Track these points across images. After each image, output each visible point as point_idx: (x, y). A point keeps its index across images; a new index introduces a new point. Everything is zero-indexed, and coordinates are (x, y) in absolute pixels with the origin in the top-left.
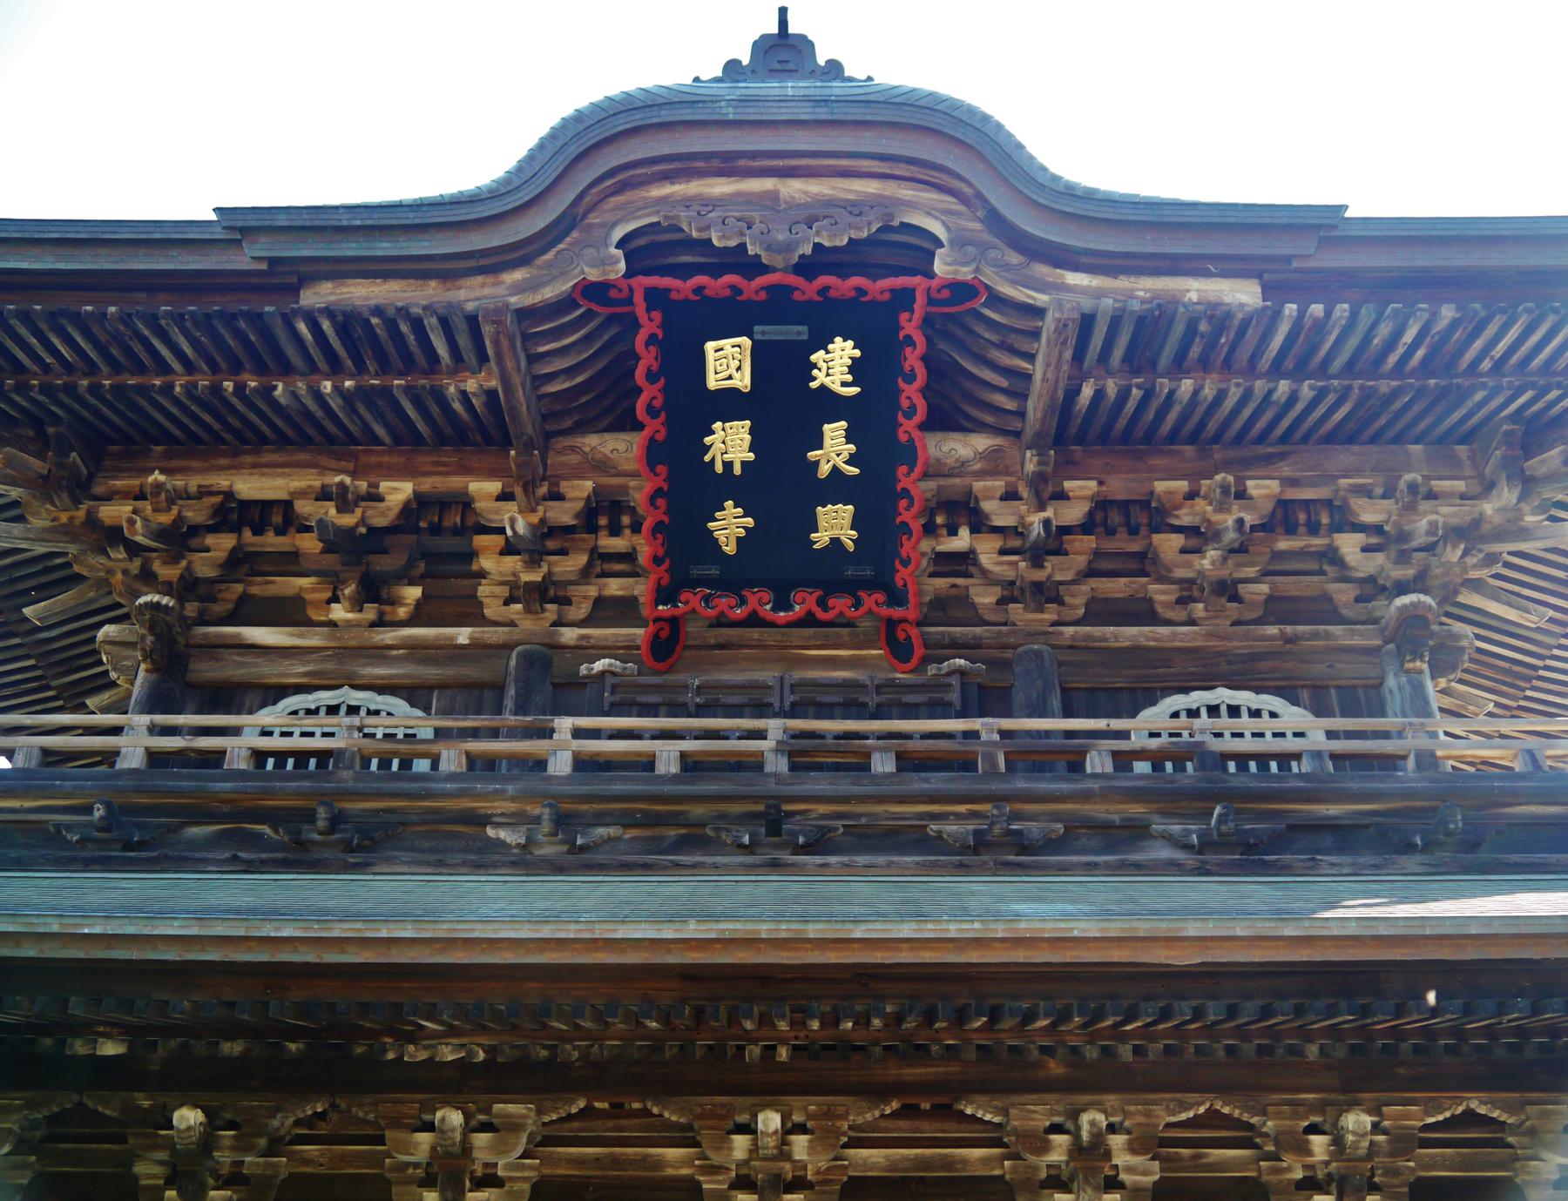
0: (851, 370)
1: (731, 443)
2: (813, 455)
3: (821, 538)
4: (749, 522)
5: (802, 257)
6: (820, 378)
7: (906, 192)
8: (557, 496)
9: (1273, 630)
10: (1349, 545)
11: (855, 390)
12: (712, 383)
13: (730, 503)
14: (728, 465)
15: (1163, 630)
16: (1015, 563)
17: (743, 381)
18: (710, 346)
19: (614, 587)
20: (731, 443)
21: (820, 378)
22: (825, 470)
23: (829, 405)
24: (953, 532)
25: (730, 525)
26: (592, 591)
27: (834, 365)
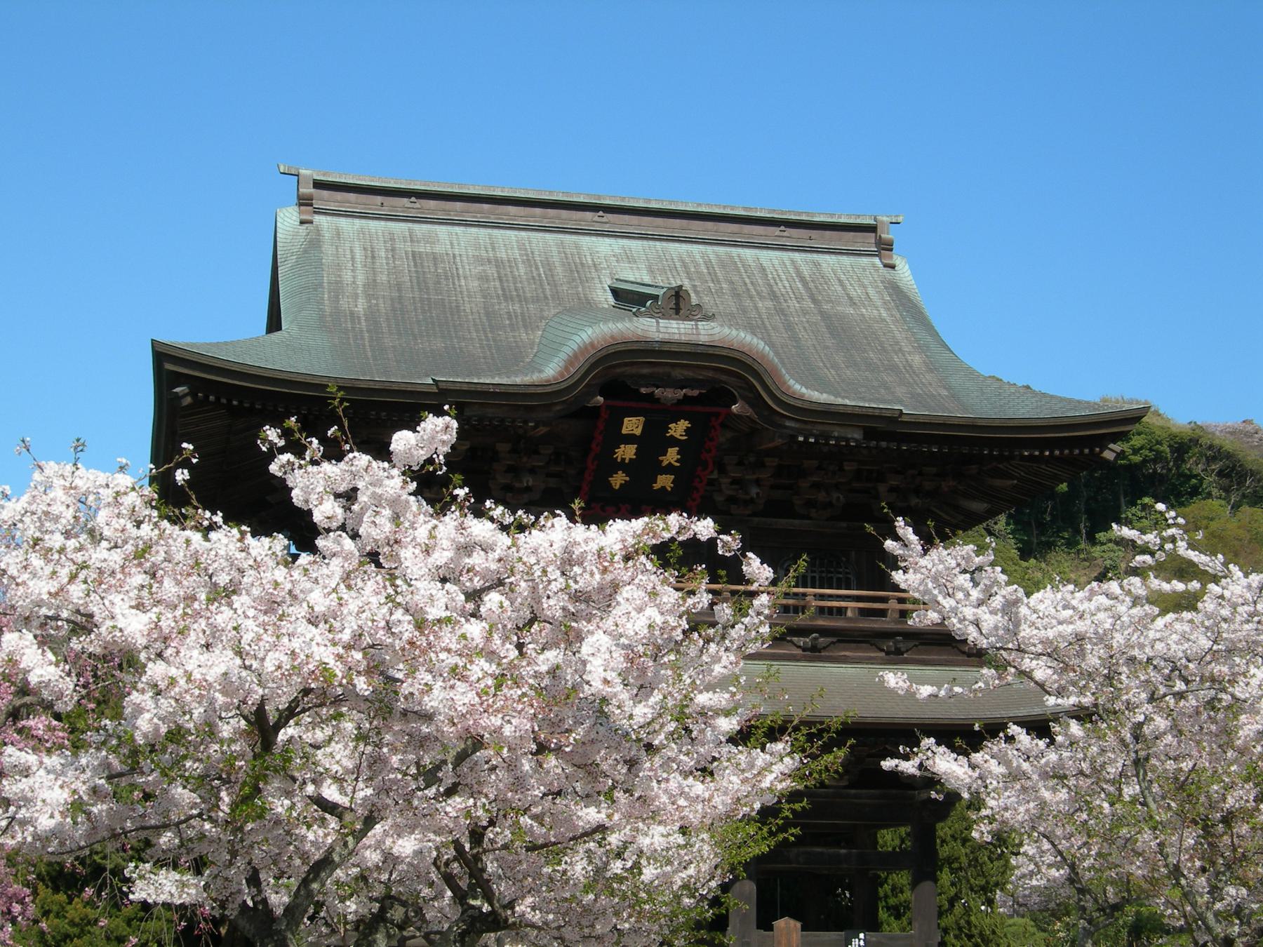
1: (627, 452)
3: (656, 486)
6: (671, 432)
7: (724, 378)
8: (536, 452)
9: (844, 524)
10: (882, 488)
12: (624, 431)
14: (623, 459)
15: (797, 522)
17: (638, 432)
18: (626, 419)
19: (552, 482)
21: (671, 432)
22: (665, 463)
23: (673, 442)
25: (618, 479)
27: (679, 429)
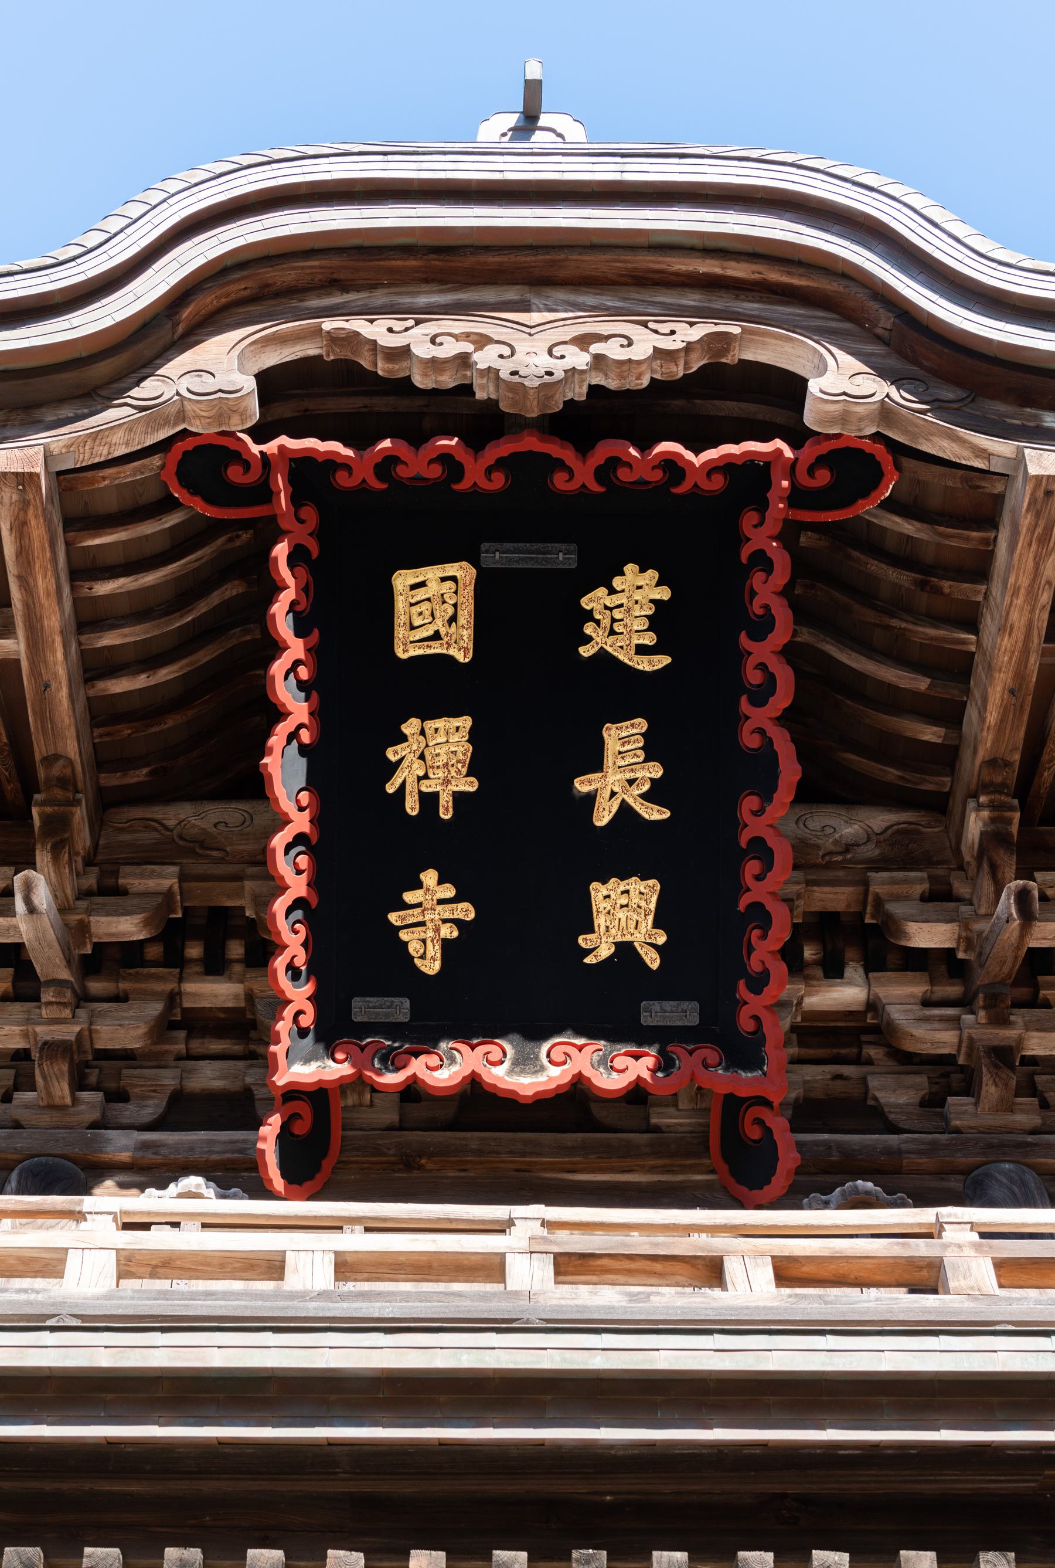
0: (655, 623)
1: (434, 759)
2: (582, 785)
3: (599, 947)
4: (466, 911)
5: (570, 404)
11: (662, 661)
12: (407, 647)
13: (430, 877)
14: (429, 801)
16: (957, 1019)
18: (402, 580)
20: (434, 759)
23: (614, 690)
24: (834, 971)
25: (430, 918)
26: (169, 1079)
